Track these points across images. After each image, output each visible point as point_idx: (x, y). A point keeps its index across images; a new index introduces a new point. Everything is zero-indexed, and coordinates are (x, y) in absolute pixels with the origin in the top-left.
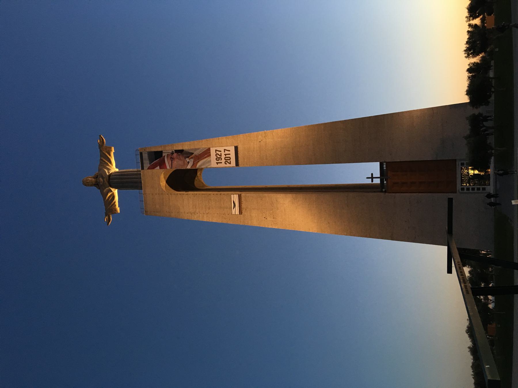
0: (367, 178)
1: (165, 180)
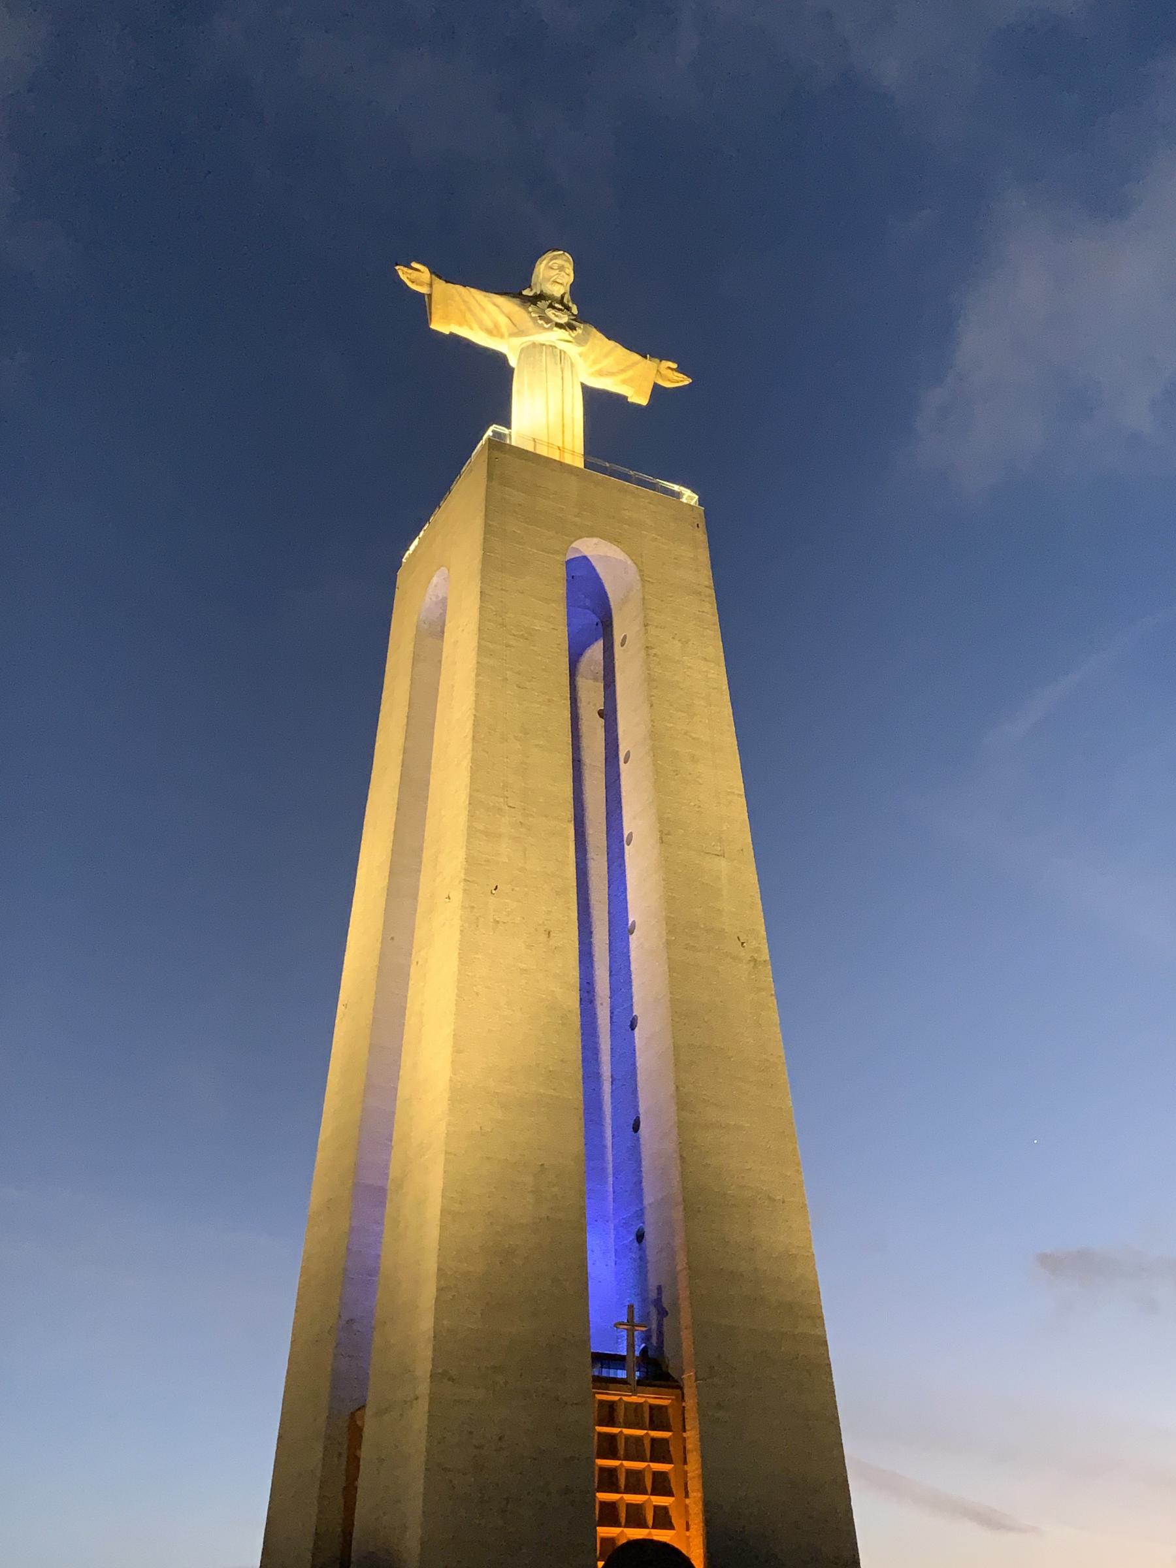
1: (592, 556)
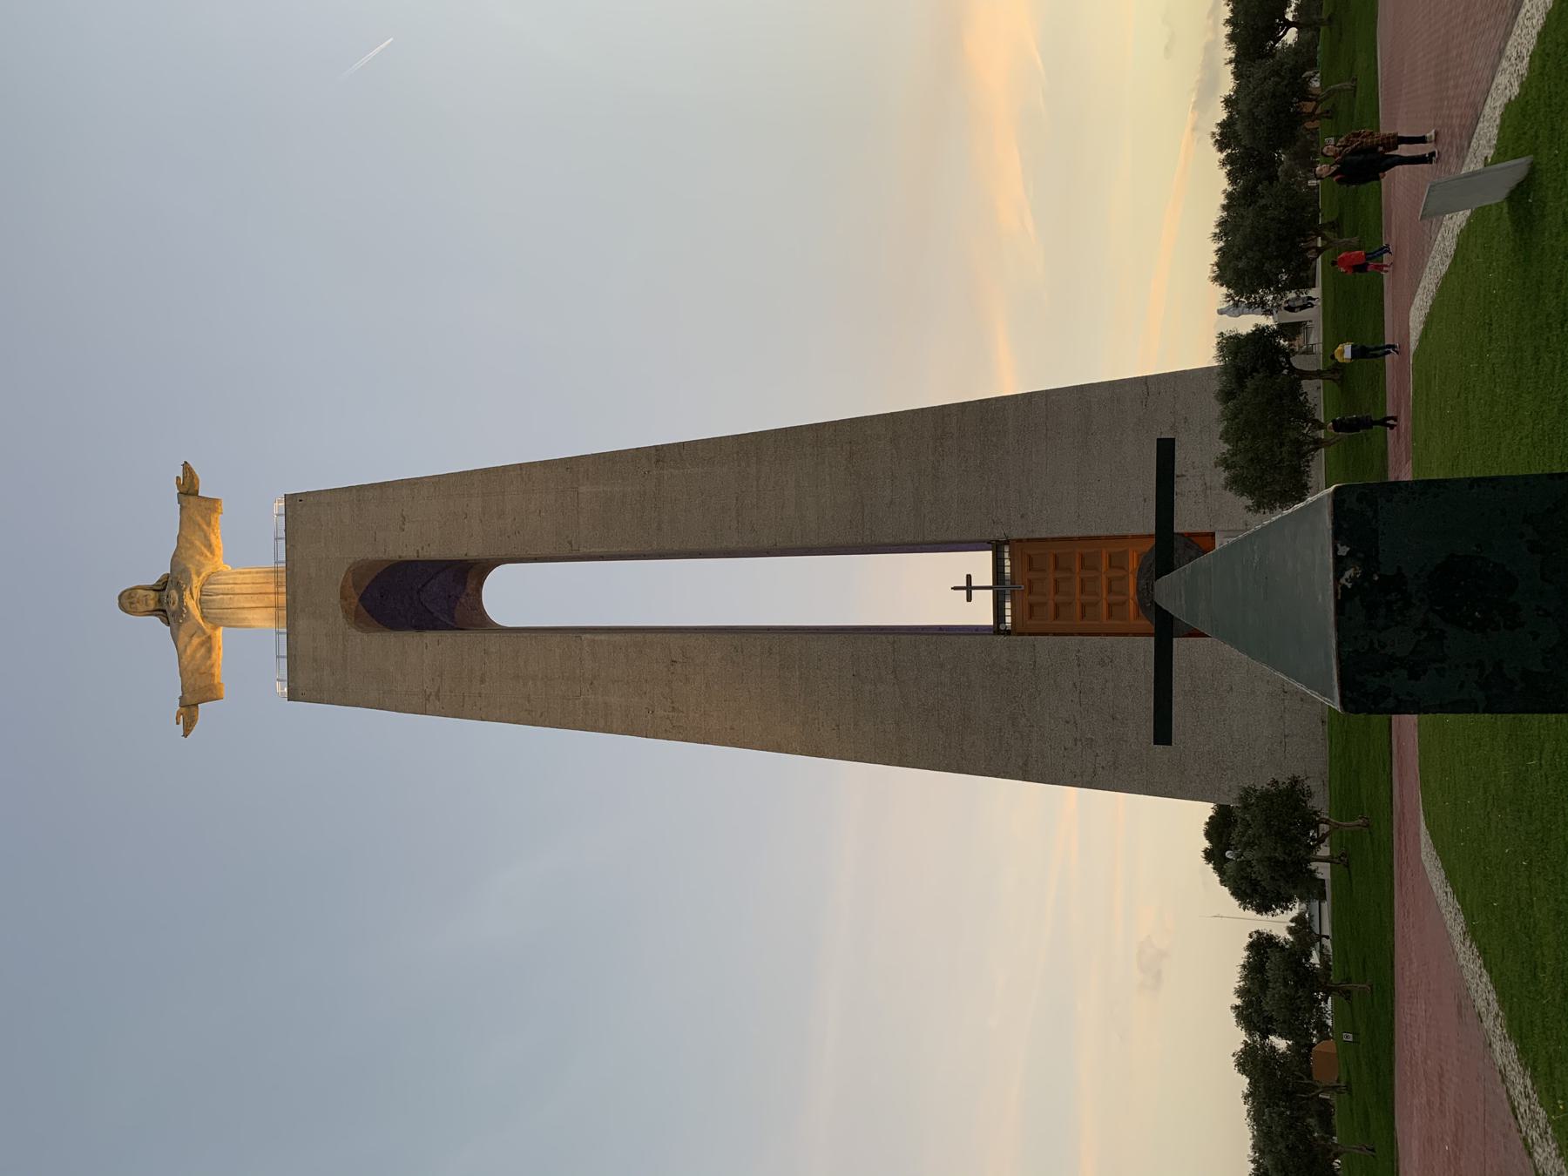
0: (955, 588)
1: (358, 594)
